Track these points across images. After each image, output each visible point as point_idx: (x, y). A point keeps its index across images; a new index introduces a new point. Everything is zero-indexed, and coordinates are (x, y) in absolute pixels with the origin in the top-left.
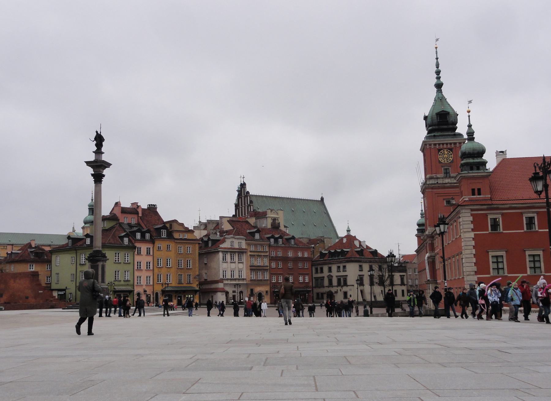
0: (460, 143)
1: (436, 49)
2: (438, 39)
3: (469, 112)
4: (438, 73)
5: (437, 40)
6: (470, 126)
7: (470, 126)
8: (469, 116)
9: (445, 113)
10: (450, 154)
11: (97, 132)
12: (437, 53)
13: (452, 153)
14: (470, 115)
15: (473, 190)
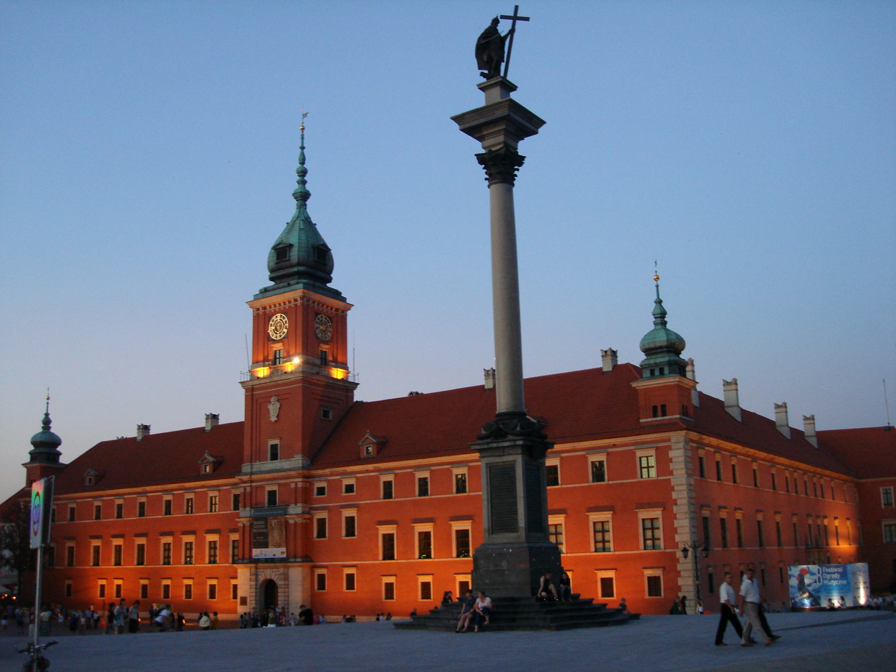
0: (343, 312)
1: (303, 132)
2: (306, 114)
3: (657, 279)
4: (303, 173)
5: (305, 115)
6: (659, 302)
7: (659, 302)
8: (657, 286)
9: (324, 248)
10: (284, 321)
11: (496, 22)
12: (303, 138)
13: (332, 324)
14: (659, 284)
15: (655, 408)
